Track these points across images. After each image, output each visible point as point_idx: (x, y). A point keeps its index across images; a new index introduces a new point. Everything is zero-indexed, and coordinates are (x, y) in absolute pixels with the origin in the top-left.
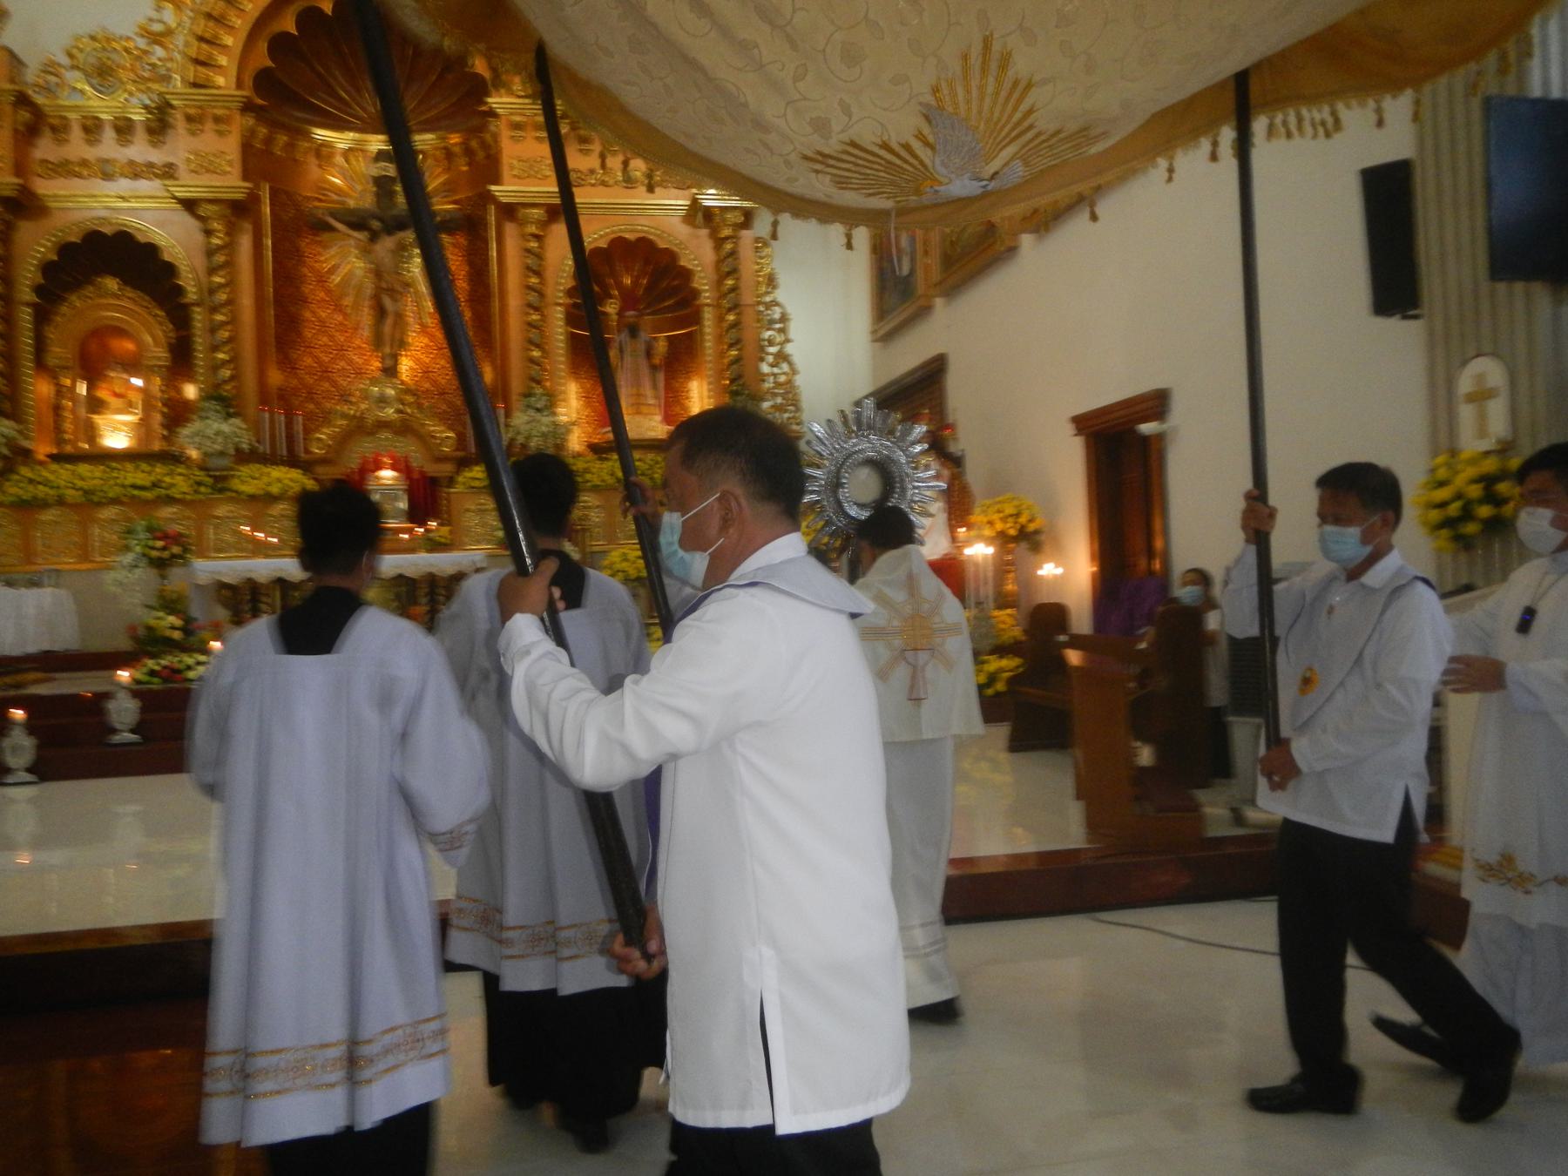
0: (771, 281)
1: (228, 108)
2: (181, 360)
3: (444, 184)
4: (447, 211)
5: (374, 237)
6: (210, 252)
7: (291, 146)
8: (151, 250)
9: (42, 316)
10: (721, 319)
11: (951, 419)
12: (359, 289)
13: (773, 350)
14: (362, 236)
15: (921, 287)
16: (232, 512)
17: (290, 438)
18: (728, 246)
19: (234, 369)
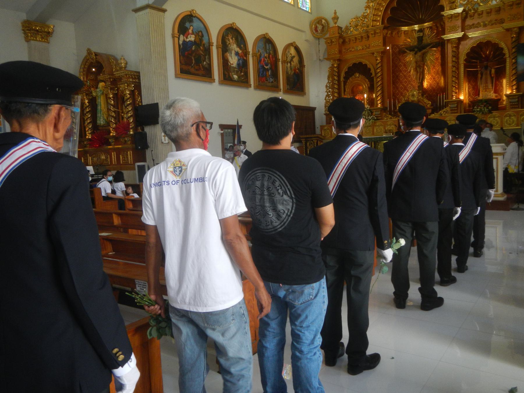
5: (416, 54)
8: (366, 65)
9: (345, 85)
14: (414, 52)
16: (379, 124)
18: (514, 39)
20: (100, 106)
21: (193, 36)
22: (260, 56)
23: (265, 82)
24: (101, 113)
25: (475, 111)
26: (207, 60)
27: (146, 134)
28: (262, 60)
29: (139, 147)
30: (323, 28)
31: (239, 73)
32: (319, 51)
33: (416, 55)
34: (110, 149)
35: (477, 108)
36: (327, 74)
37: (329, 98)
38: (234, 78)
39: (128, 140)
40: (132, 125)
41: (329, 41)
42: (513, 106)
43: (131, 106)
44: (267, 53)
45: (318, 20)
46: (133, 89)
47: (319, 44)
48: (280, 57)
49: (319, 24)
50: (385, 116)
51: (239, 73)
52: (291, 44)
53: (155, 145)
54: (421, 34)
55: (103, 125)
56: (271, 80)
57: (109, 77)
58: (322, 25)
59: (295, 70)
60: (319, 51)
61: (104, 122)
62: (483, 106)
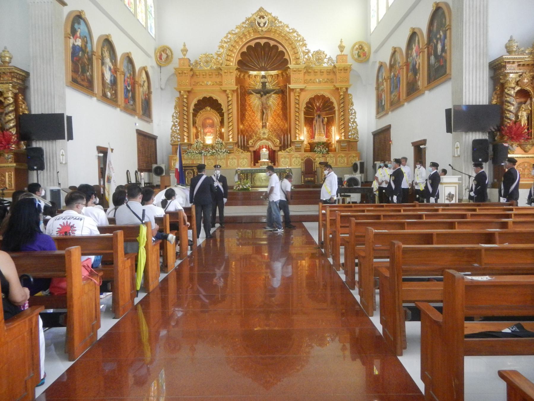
0: (352, 104)
1: (233, 70)
3: (276, 83)
4: (278, 89)
5: (262, 96)
6: (228, 102)
7: (244, 76)
8: (216, 101)
9: (195, 115)
10: (340, 113)
11: (391, 139)
13: (352, 120)
14: (259, 95)
15: (386, 108)
17: (244, 141)
21: (80, 40)
22: (125, 75)
25: (316, 151)
26: (90, 70)
30: (168, 57)
32: (161, 79)
33: (262, 98)
35: (318, 149)
36: (174, 104)
37: (176, 128)
41: (180, 72)
42: (343, 149)
43: (14, 113)
44: (129, 73)
45: (163, 48)
47: (161, 72)
49: (163, 52)
50: (236, 150)
52: (144, 69)
53: (52, 166)
54: (266, 80)
56: (132, 102)
58: (167, 54)
59: (145, 96)
60: (161, 79)
62: (322, 147)
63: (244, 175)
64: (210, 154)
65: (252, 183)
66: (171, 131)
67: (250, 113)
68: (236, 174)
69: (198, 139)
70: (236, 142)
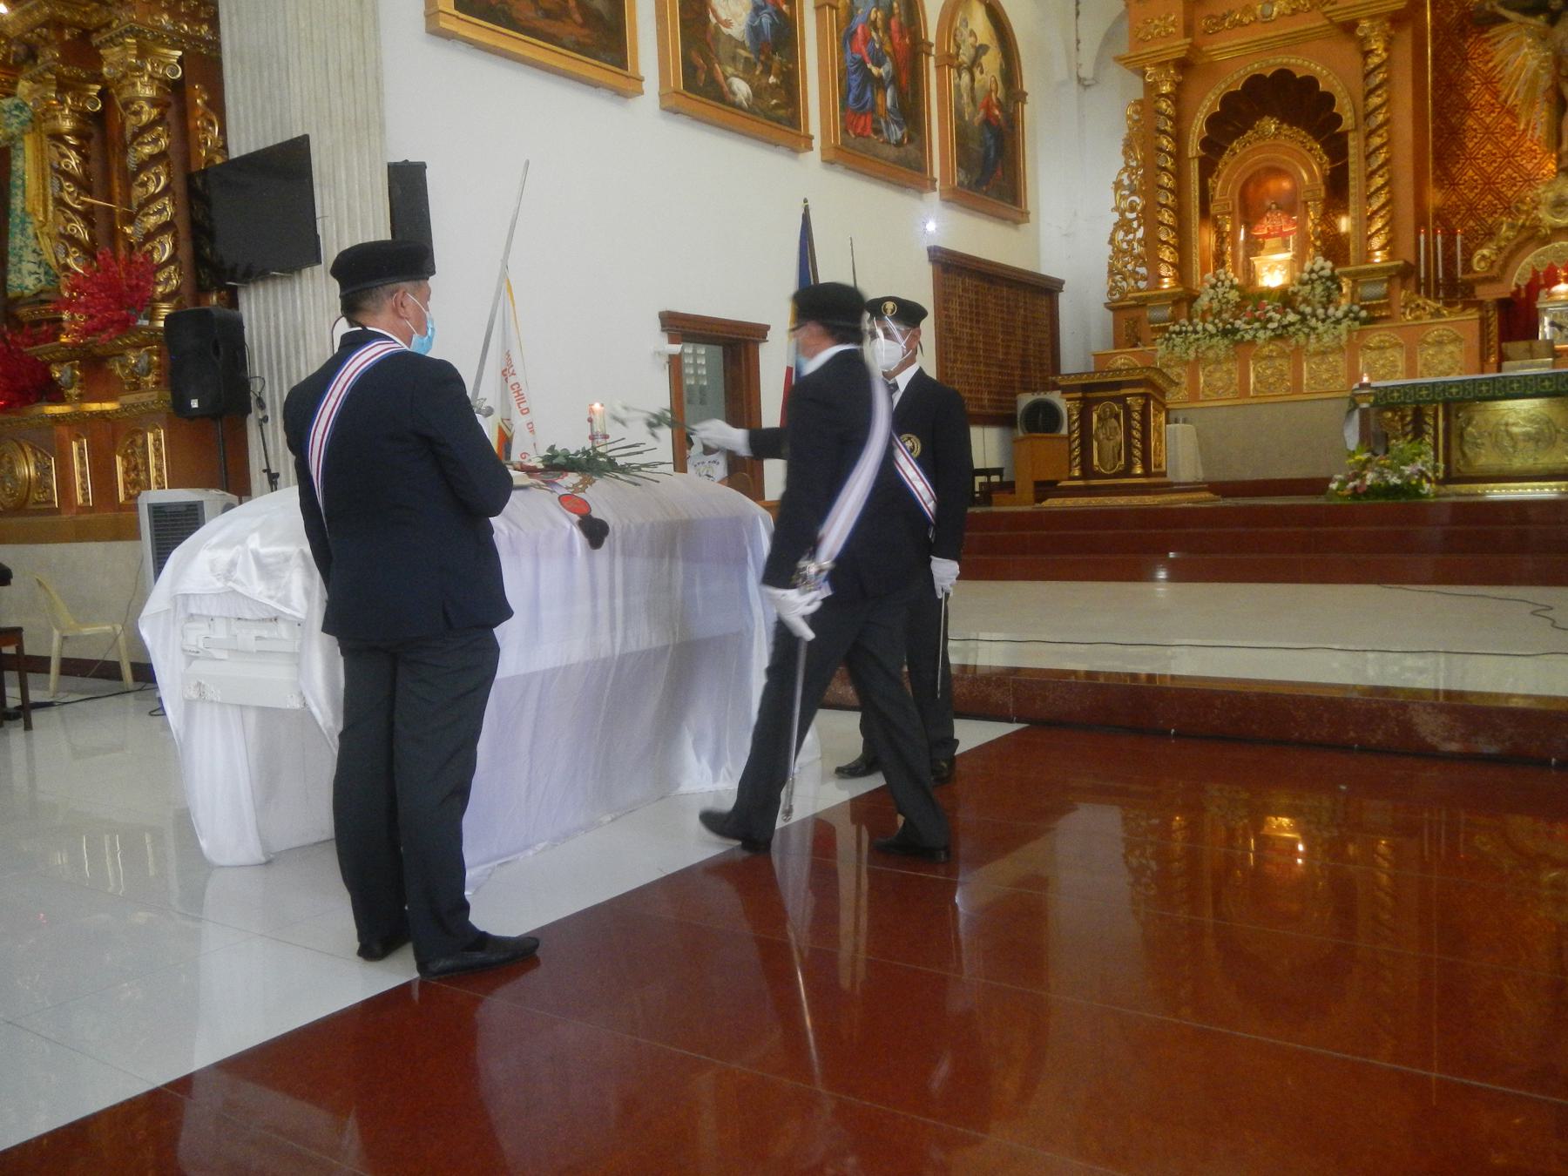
2: (1337, 190)
8: (1310, 82)
12: (1532, 84)
16: (1381, 341)
17: (1450, 260)
19: (1389, 192)
20: (19, 193)
23: (868, 137)
24: (23, 230)
27: (237, 326)
28: (855, 32)
29: (195, 404)
31: (757, 73)
32: (1078, 42)
34: (56, 419)
37: (1131, 236)
38: (734, 94)
39: (143, 364)
40: (169, 279)
46: (179, 76)
47: (1078, 14)
48: (932, 38)
50: (1405, 307)
51: (757, 73)
55: (36, 295)
56: (896, 133)
57: (46, 10)
59: (988, 108)
60: (1078, 42)
61: (42, 278)
63: (1403, 418)
64: (1269, 333)
65: (1447, 461)
66: (1109, 250)
67: (1488, 120)
68: (1350, 412)
69: (1218, 272)
70: (1401, 262)
